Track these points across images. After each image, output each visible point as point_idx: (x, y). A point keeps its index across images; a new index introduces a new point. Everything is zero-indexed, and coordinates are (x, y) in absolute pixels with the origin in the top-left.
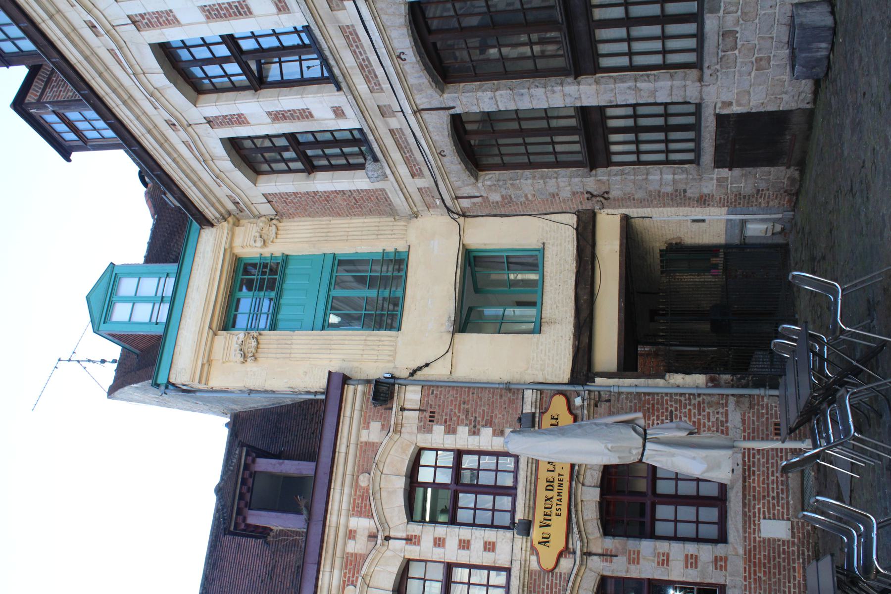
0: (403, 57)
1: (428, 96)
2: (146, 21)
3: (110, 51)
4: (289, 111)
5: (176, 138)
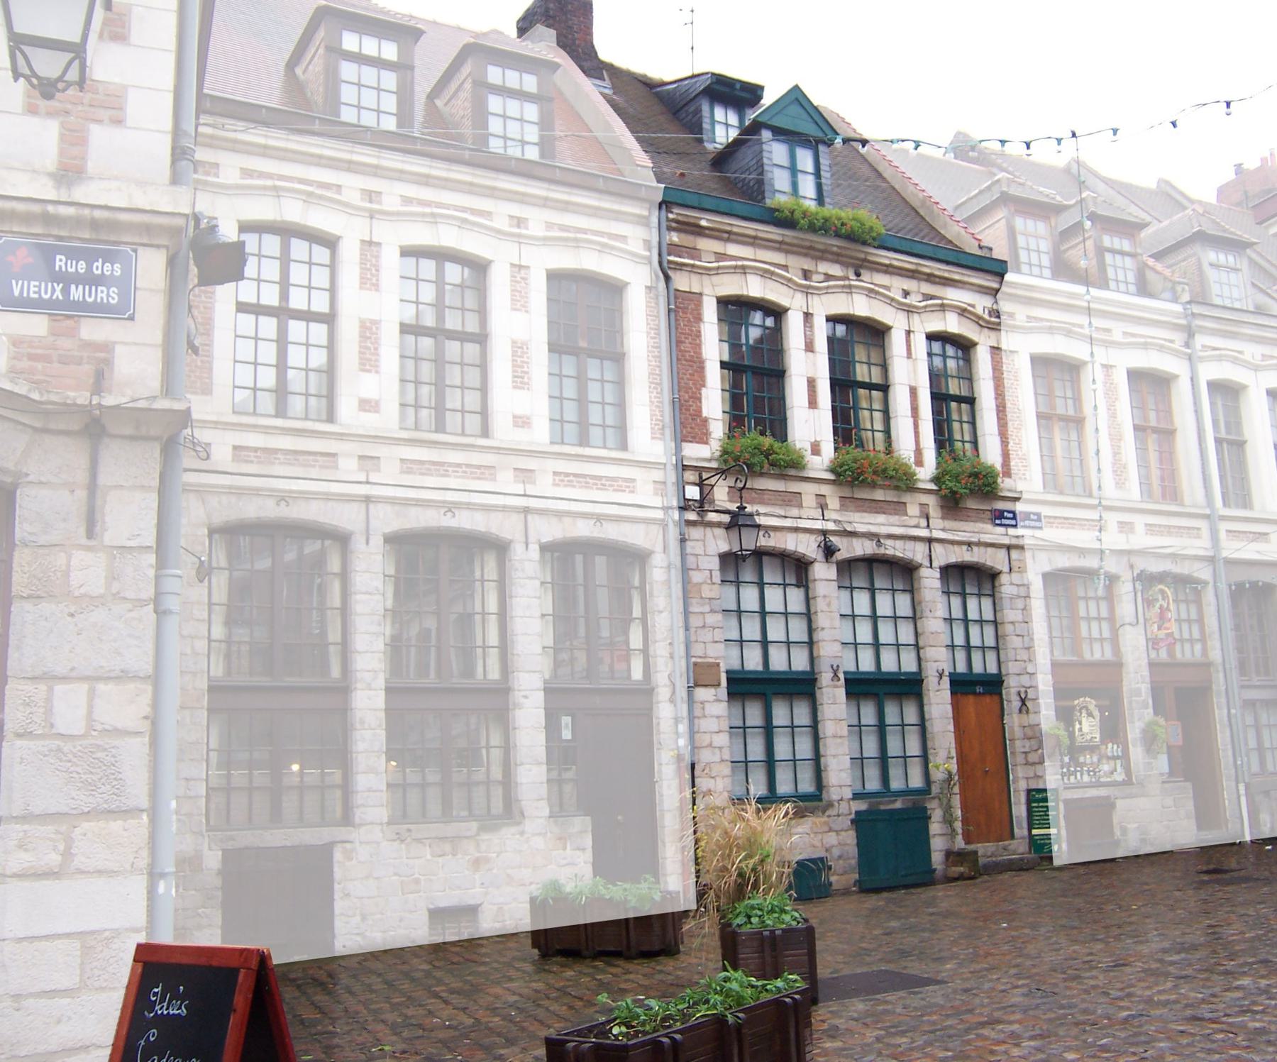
0: (449, 514)
1: (388, 521)
2: (518, 279)
3: (488, 214)
4: (376, 349)
5: (353, 185)
